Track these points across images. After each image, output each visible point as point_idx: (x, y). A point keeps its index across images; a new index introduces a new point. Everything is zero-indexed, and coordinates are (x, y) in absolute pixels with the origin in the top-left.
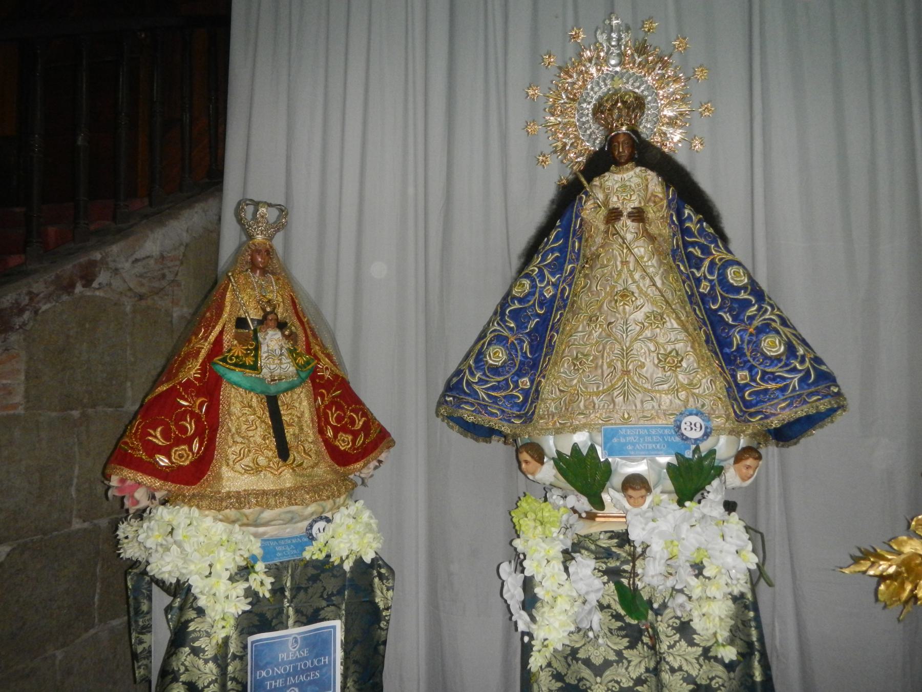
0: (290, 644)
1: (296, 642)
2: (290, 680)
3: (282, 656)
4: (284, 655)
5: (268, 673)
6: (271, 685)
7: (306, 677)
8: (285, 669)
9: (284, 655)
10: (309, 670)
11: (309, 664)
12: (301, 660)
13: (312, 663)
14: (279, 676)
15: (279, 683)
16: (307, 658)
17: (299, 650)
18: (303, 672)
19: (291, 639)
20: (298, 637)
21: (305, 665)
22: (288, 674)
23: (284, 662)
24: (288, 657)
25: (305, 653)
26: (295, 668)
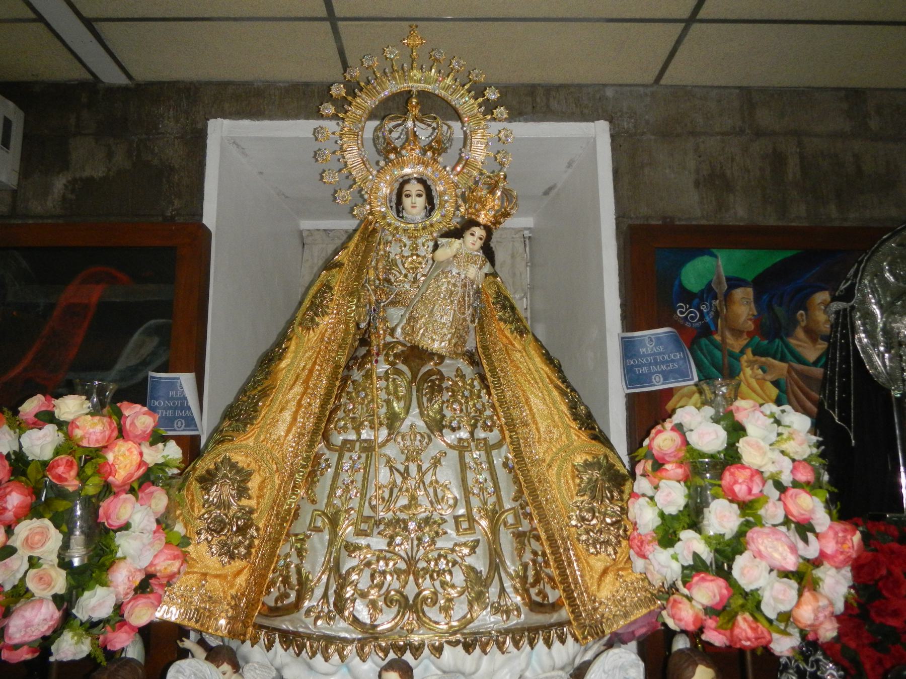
0: (647, 342)
1: (651, 340)
2: (654, 369)
3: (642, 351)
4: (644, 350)
5: (634, 362)
6: (639, 371)
7: (667, 367)
8: (647, 360)
9: (644, 350)
10: (667, 362)
11: (666, 357)
12: (659, 354)
13: (669, 357)
14: (645, 365)
15: (645, 370)
16: (663, 353)
17: (655, 346)
18: (663, 363)
19: (646, 338)
20: (652, 337)
21: (663, 358)
22: (650, 364)
23: (644, 356)
24: (647, 351)
25: (661, 349)
26: (655, 359)
